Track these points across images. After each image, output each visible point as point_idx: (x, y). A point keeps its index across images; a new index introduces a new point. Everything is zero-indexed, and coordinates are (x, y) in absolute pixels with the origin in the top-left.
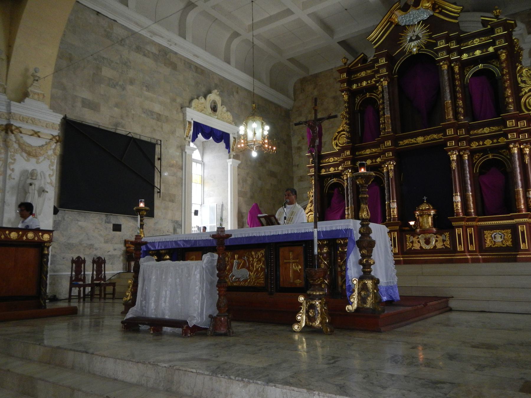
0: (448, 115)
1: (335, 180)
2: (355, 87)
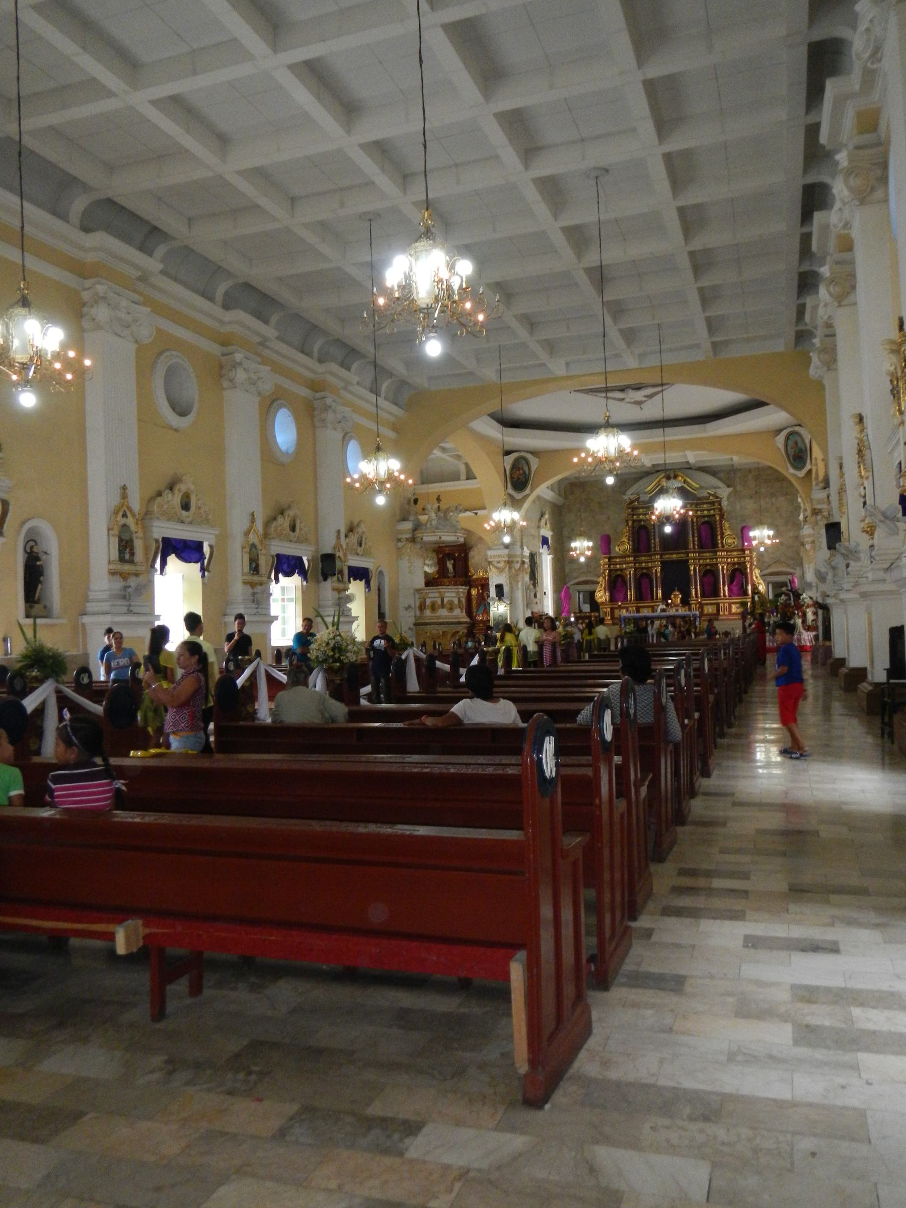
1: (619, 572)
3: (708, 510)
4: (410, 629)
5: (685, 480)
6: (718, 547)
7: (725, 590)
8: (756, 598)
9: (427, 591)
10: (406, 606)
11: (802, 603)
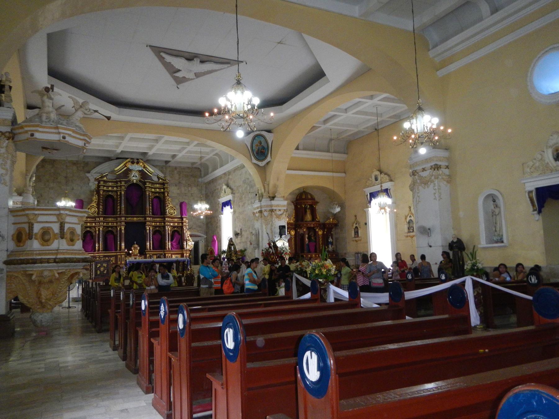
1: (88, 229)
2: (105, 188)
5: (144, 166)
6: (166, 215)
7: (169, 245)
9: (37, 212)
11: (282, 251)
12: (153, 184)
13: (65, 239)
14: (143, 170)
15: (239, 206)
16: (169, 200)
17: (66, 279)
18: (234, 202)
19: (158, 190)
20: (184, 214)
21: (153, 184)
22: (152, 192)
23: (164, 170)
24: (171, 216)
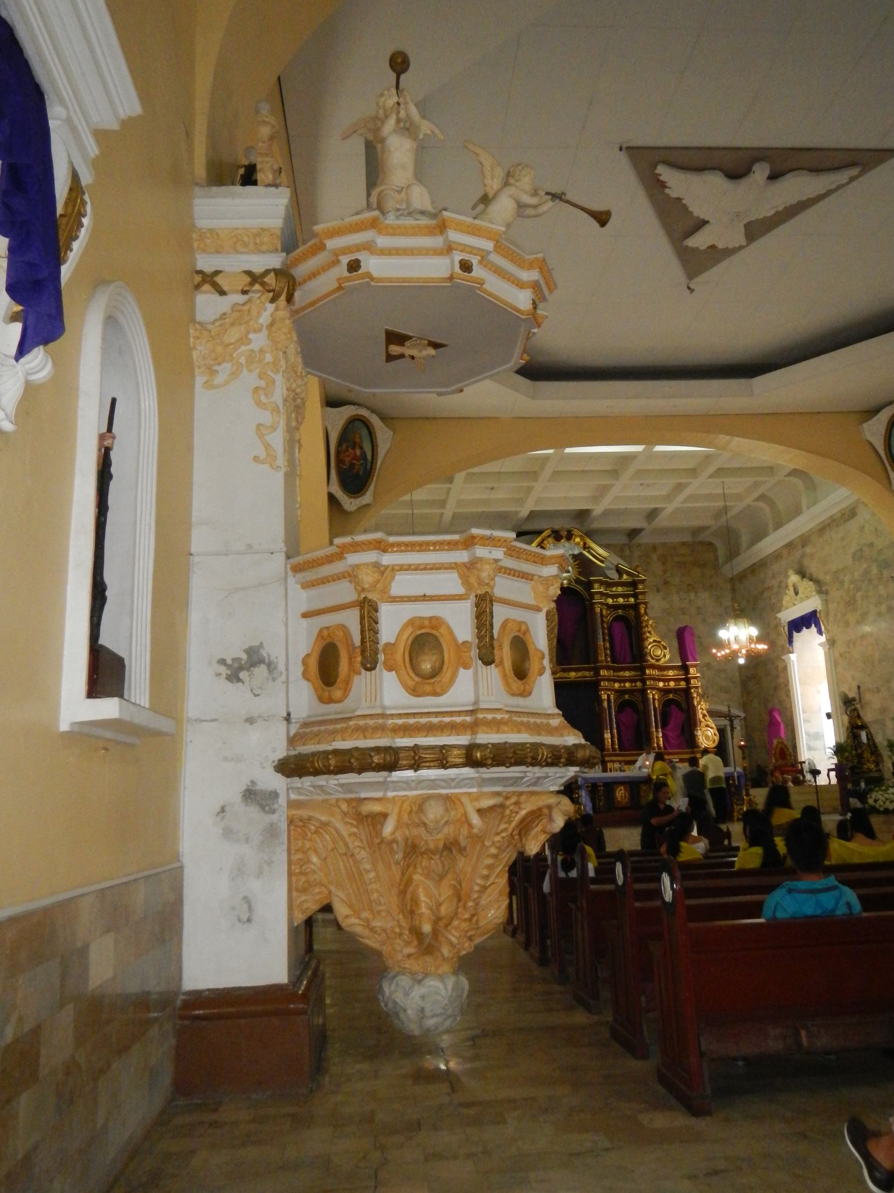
0: (602, 656)
3: (623, 596)
4: (251, 794)
5: (585, 544)
8: (864, 738)
10: (236, 652)
12: (609, 585)
13: (497, 666)
14: (581, 554)
15: (847, 623)
16: (649, 622)
17: (504, 834)
18: (827, 614)
19: (621, 600)
20: (690, 658)
21: (609, 585)
22: (609, 607)
23: (627, 553)
24: (657, 663)
